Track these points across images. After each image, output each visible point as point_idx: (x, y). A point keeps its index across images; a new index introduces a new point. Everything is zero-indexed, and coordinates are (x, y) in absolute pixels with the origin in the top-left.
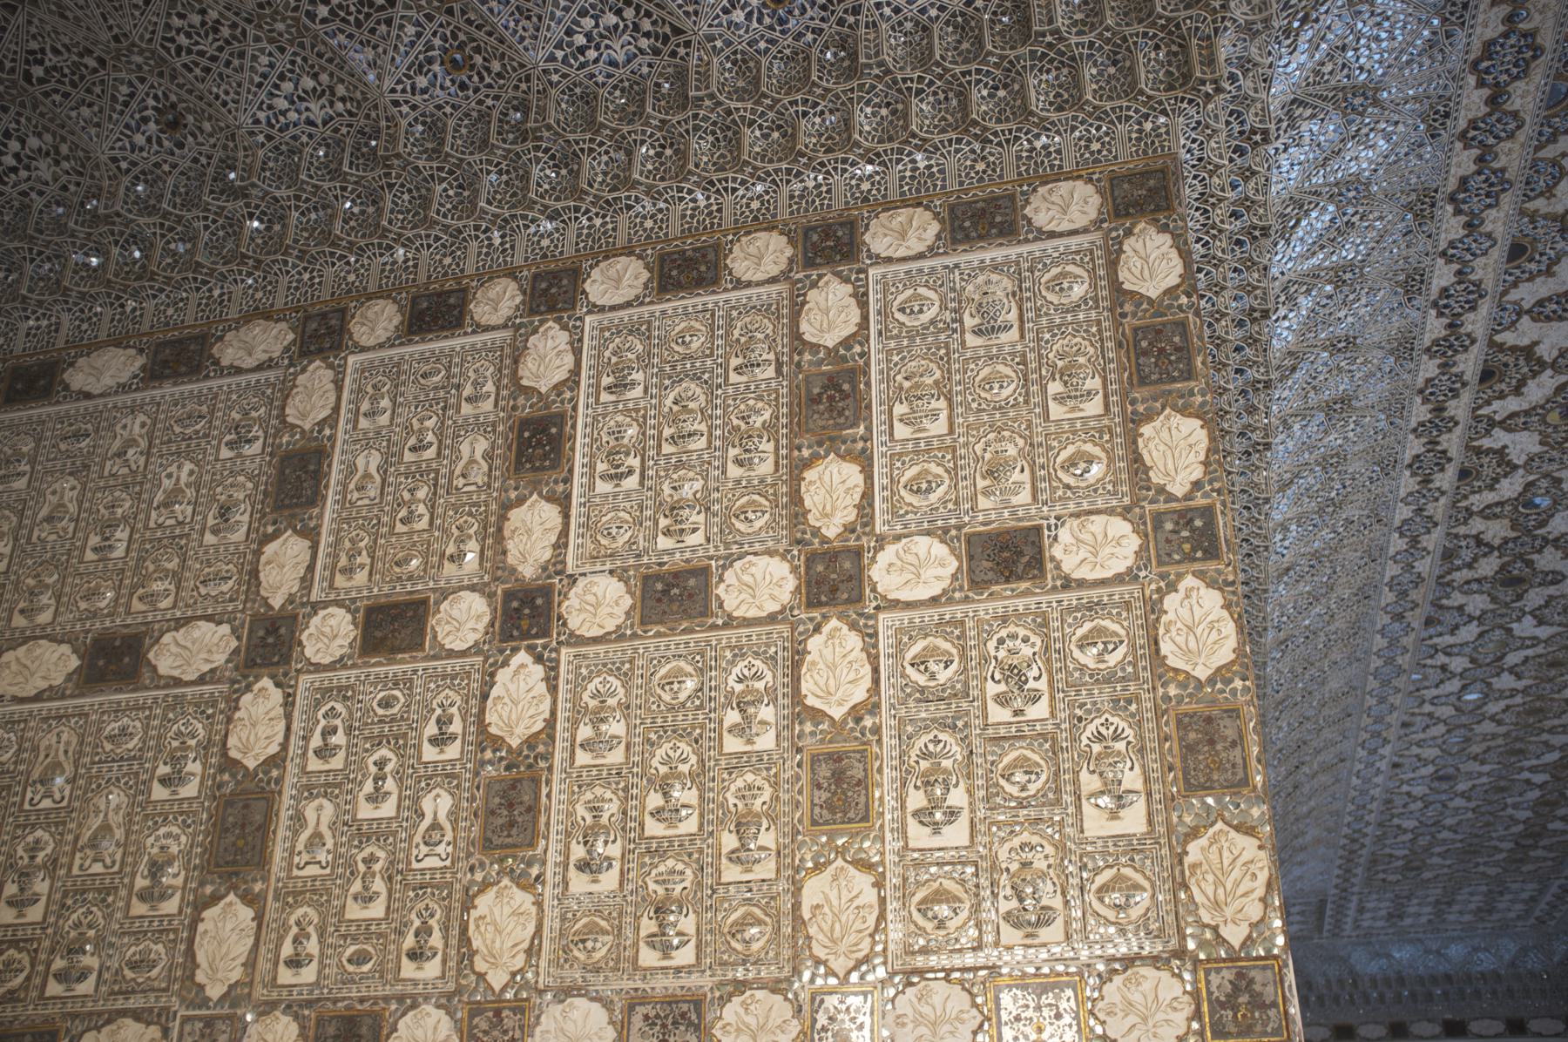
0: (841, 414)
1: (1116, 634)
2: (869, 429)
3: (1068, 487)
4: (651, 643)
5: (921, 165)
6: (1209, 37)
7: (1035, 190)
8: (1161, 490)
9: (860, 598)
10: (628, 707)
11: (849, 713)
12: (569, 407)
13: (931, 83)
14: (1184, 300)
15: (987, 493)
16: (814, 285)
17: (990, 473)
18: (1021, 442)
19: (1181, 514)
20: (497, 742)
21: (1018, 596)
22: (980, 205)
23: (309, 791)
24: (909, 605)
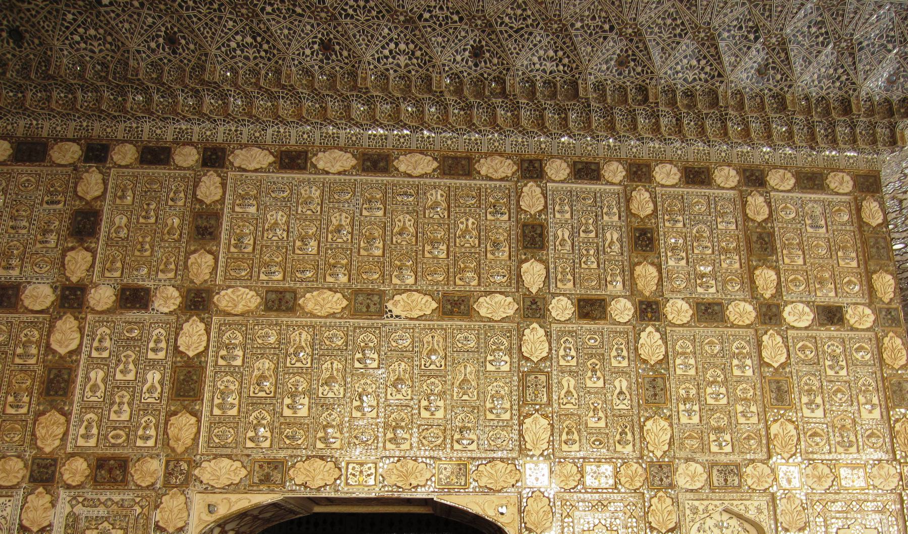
4: (701, 330)
12: (654, 226)
16: (750, 194)
19: (888, 309)
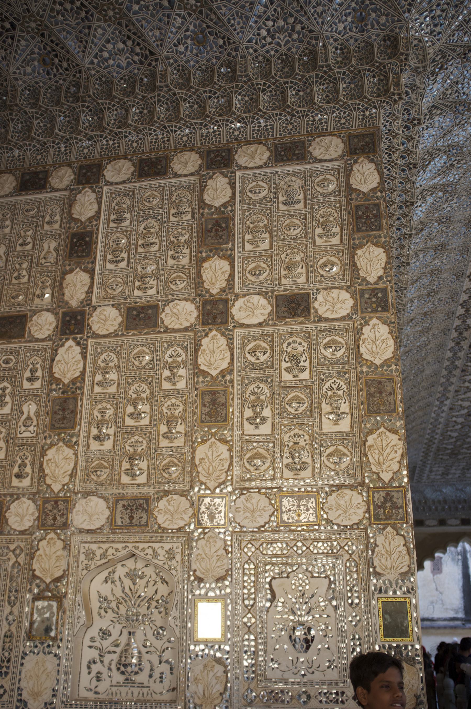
0: (221, 238)
1: (340, 343)
2: (233, 245)
3: (322, 276)
4: (130, 338)
5: (263, 125)
6: (398, 73)
7: (314, 140)
8: (364, 279)
9: (226, 322)
10: (119, 367)
11: (219, 373)
12: (95, 228)
13: (269, 86)
14: (379, 194)
15: (286, 277)
16: (211, 178)
17: (288, 268)
18: (302, 255)
19: (373, 291)
20: (58, 381)
21: (298, 324)
22: (288, 145)
24: (248, 326)
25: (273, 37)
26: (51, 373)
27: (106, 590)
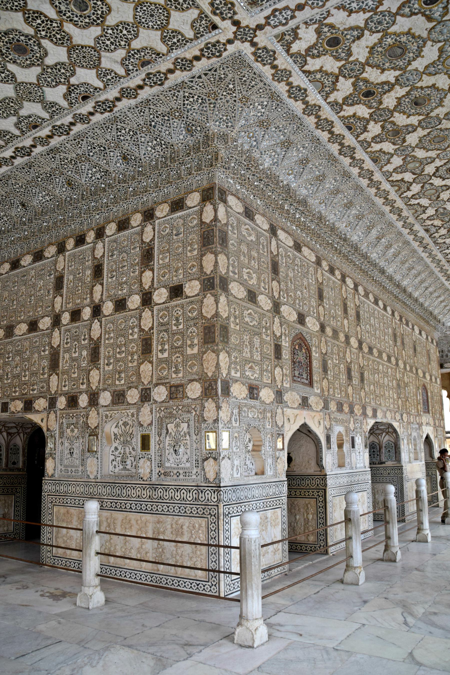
8: (205, 273)
9: (151, 304)
17: (176, 271)
23: (65, 352)
24: (159, 304)
25: (154, 149)
26: (90, 336)
27: (116, 431)
